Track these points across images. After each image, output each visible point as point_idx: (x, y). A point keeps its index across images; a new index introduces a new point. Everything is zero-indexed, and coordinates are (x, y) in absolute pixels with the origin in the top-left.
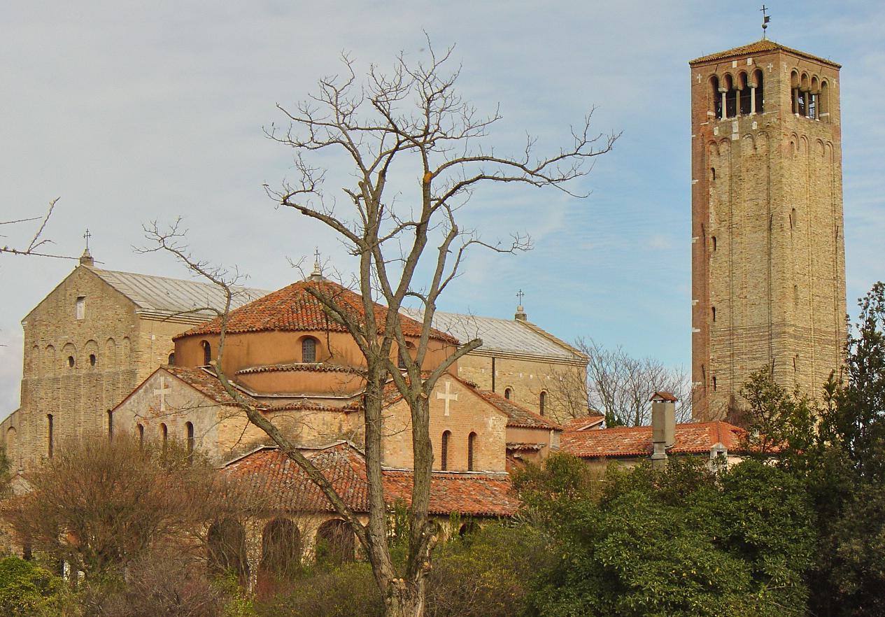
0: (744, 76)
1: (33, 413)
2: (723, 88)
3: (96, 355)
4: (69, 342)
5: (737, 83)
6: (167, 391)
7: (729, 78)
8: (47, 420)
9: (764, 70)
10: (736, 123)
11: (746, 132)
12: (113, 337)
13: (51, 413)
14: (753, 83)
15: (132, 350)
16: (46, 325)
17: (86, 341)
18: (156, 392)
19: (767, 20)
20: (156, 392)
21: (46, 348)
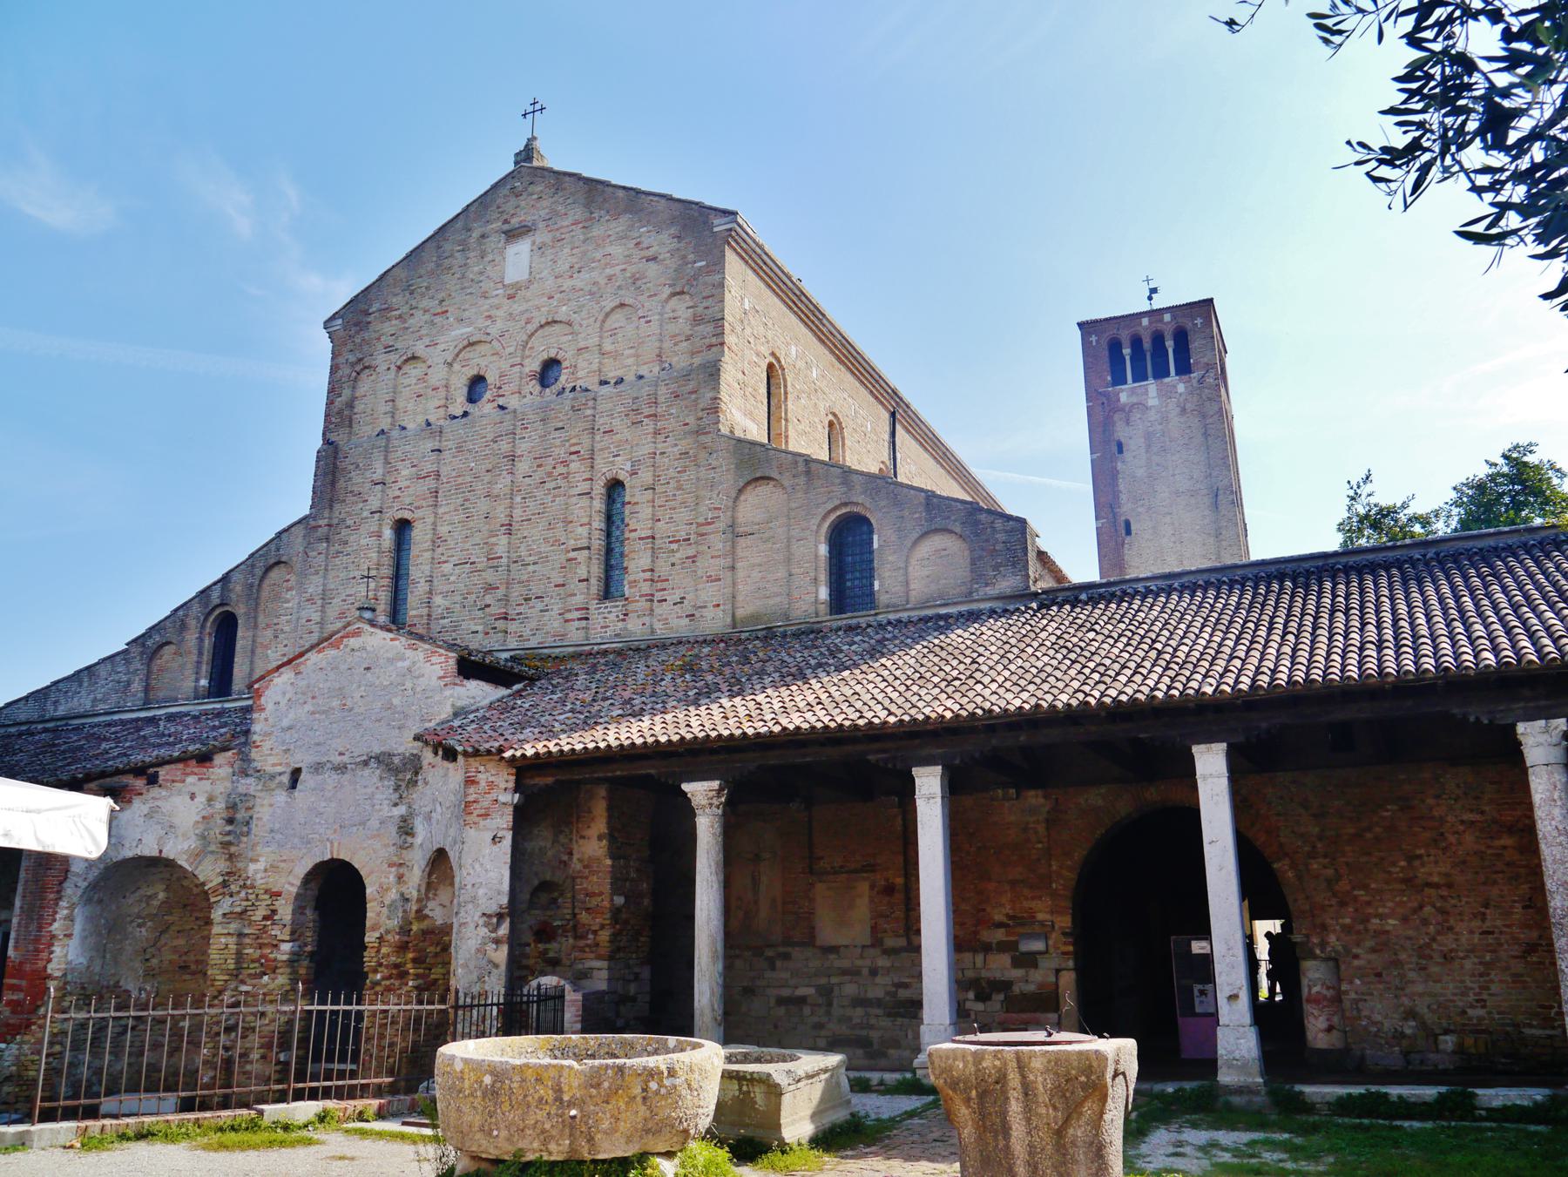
0: (1158, 339)
1: (349, 522)
2: (1127, 351)
3: (568, 358)
4: (473, 339)
5: (1147, 345)
7: (1136, 342)
8: (388, 534)
9: (1189, 326)
10: (1151, 386)
11: (1165, 394)
12: (629, 301)
13: (407, 515)
14: (1170, 344)
15: (697, 320)
16: (400, 316)
17: (531, 328)
19: (1154, 291)
21: (399, 368)
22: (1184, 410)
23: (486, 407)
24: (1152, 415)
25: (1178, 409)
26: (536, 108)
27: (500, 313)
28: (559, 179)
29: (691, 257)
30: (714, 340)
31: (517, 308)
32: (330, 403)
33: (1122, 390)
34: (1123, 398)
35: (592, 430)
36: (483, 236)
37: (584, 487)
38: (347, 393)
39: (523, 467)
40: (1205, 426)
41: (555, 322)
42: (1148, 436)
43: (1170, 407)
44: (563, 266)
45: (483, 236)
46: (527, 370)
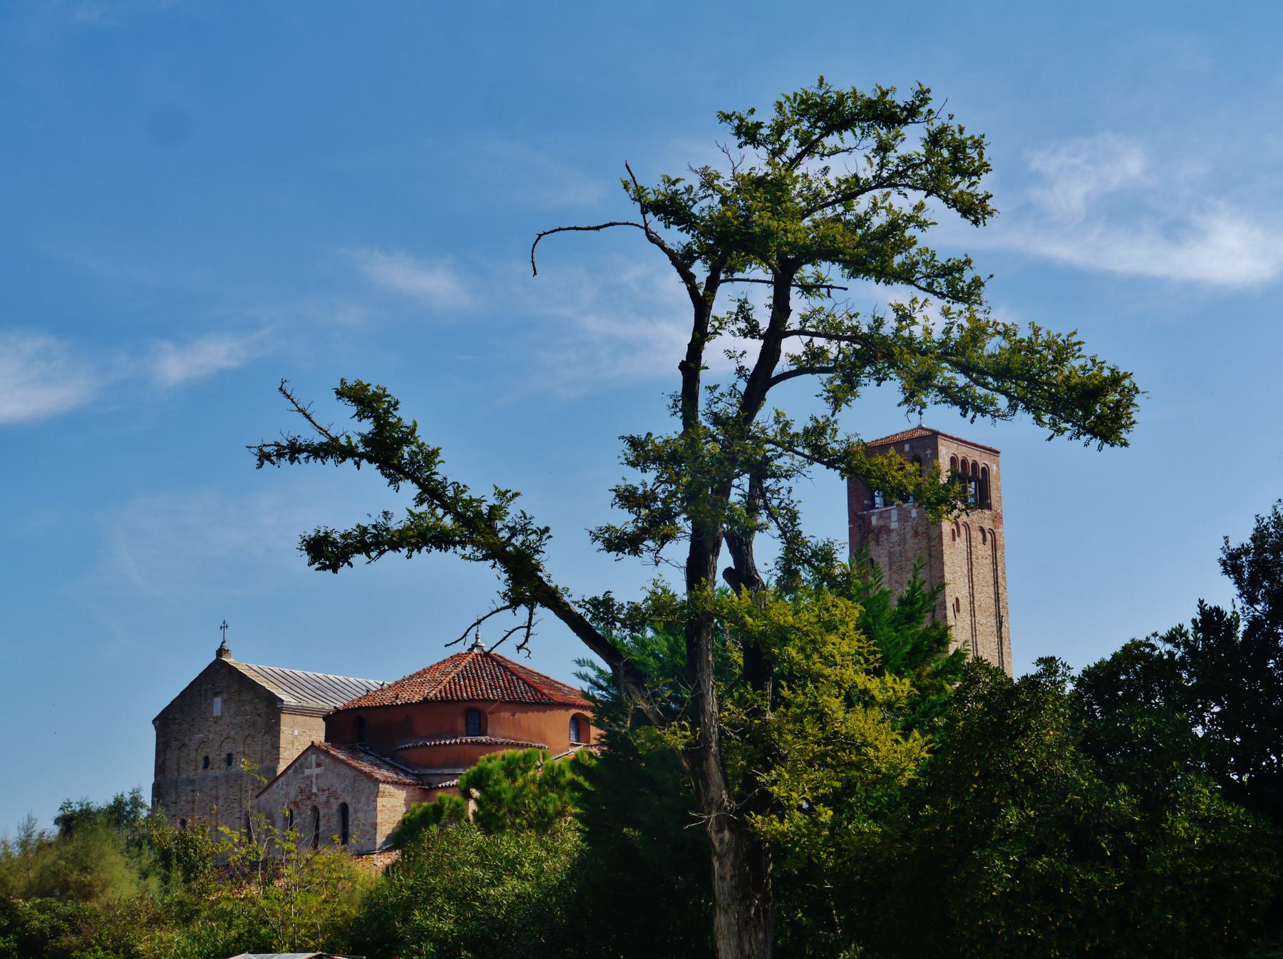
6: (318, 771)
9: (922, 455)
16: (179, 724)
17: (222, 738)
18: (307, 772)
20: (307, 772)
21: (180, 748)
22: (916, 534)
23: (210, 772)
24: (894, 537)
25: (912, 532)
26: (224, 627)
27: (211, 729)
28: (232, 670)
29: (271, 717)
30: (276, 757)
31: (218, 729)
32: (156, 761)
33: (874, 514)
34: (874, 521)
35: (241, 790)
36: (206, 690)
37: (238, 815)
38: (162, 757)
39: (221, 802)
40: (929, 547)
41: (229, 737)
42: (891, 555)
43: (908, 529)
44: (232, 711)
45: (206, 690)
46: (222, 757)
